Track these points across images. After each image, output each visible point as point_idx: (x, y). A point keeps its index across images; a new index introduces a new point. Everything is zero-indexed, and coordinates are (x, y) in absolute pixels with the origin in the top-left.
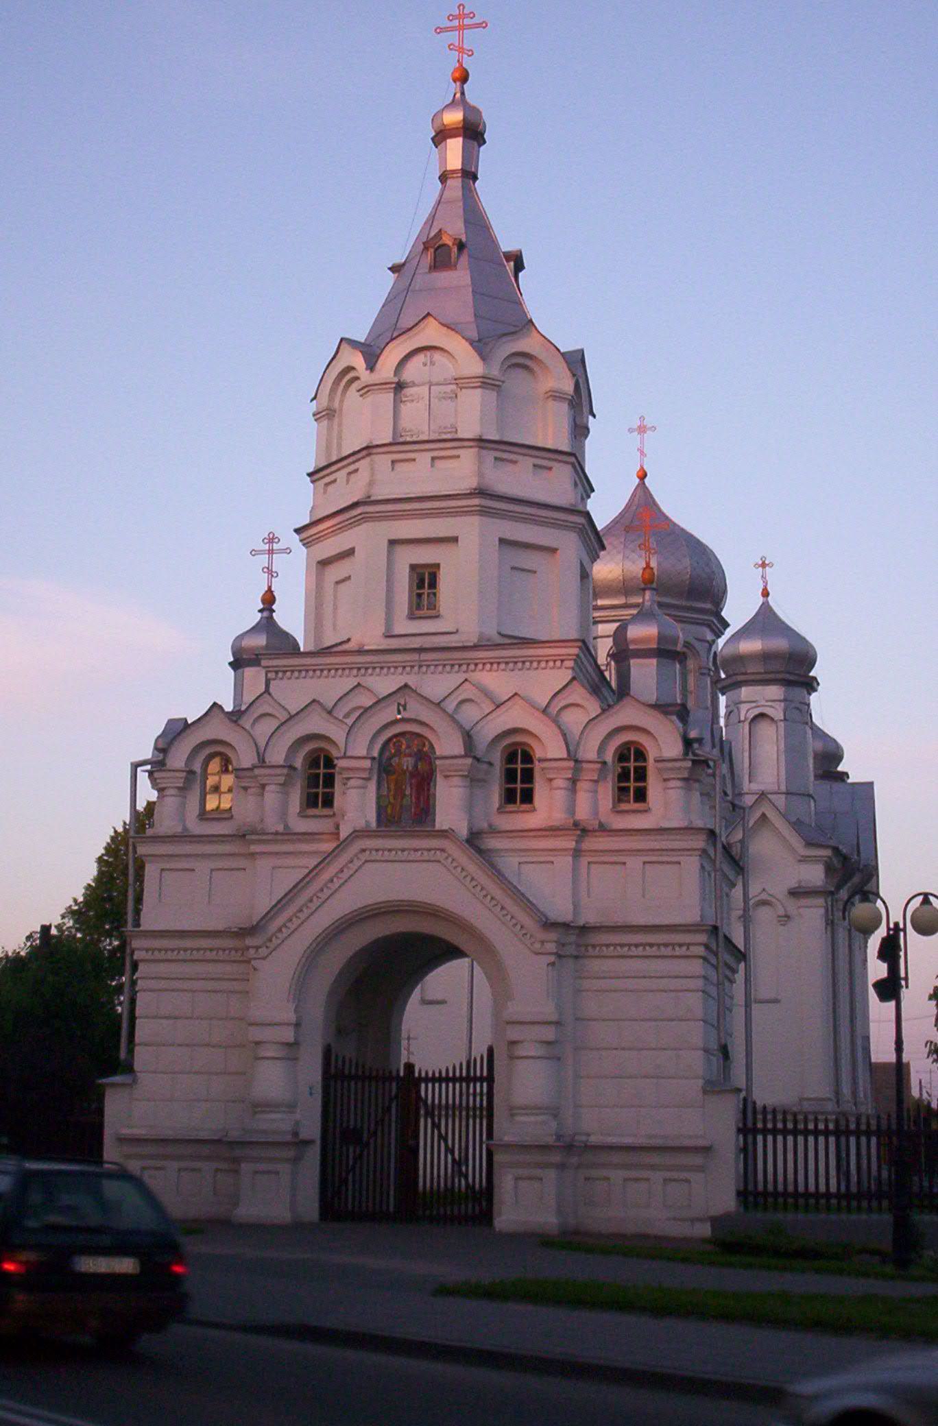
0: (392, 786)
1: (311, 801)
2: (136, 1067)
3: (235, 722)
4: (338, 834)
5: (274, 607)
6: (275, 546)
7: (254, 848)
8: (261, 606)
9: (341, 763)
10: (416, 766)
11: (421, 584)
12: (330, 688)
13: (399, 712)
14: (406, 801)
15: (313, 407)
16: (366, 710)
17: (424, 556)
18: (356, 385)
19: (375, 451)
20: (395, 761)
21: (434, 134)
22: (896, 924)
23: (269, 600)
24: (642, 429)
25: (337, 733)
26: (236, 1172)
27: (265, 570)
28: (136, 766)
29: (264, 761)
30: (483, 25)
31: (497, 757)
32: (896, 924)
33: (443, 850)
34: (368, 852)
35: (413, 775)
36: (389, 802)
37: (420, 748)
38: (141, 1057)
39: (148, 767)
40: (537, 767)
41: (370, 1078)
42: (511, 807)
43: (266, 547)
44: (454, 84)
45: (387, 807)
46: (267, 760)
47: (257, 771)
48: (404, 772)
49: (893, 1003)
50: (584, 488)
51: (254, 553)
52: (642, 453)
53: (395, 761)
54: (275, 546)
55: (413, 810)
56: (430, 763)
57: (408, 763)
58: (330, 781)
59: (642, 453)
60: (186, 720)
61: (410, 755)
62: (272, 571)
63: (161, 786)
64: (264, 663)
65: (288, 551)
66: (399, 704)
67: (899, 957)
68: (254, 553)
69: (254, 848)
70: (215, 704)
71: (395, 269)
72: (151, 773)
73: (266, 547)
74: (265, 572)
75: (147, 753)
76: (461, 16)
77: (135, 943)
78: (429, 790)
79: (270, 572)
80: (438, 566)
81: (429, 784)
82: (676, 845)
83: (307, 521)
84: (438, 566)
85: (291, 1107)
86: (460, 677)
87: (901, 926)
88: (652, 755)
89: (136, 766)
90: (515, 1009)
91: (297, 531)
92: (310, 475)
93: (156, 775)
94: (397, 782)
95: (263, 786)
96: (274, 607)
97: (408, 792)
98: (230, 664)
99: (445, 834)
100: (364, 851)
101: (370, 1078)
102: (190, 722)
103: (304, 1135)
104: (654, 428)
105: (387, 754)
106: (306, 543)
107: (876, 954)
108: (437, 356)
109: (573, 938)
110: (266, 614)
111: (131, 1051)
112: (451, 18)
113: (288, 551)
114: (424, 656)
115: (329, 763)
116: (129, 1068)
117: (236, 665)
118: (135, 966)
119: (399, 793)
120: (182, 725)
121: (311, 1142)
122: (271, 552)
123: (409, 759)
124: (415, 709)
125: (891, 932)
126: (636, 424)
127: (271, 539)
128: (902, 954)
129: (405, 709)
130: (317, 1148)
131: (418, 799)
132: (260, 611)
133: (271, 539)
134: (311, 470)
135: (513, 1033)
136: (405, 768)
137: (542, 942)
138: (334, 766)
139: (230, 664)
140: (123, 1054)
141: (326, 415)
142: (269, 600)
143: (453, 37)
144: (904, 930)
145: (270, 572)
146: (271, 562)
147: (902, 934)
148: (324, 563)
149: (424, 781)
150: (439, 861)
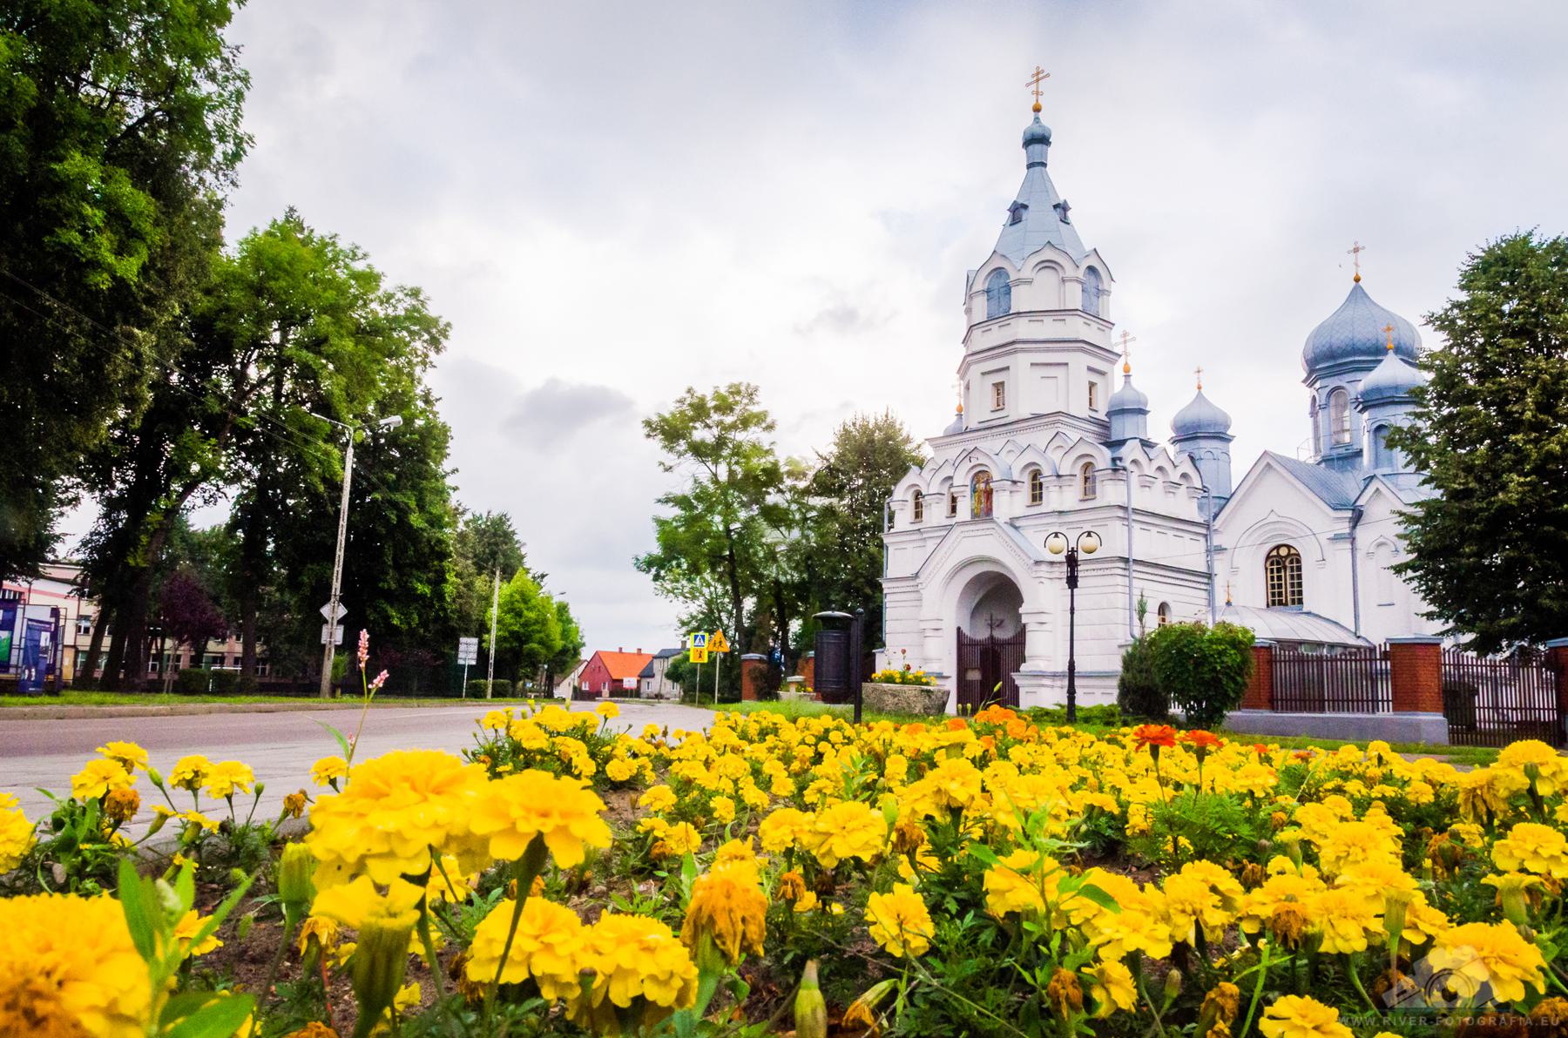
7: (925, 536)
17: (997, 378)
24: (1356, 250)
30: (1048, 75)
52: (1357, 265)
57: (982, 486)
59: (1357, 265)
69: (925, 536)
76: (1038, 73)
104: (1363, 248)
112: (1033, 76)
116: (884, 645)
119: (979, 502)
121: (947, 677)
126: (1360, 245)
141: (968, 311)
143: (1033, 87)
149: (989, 494)
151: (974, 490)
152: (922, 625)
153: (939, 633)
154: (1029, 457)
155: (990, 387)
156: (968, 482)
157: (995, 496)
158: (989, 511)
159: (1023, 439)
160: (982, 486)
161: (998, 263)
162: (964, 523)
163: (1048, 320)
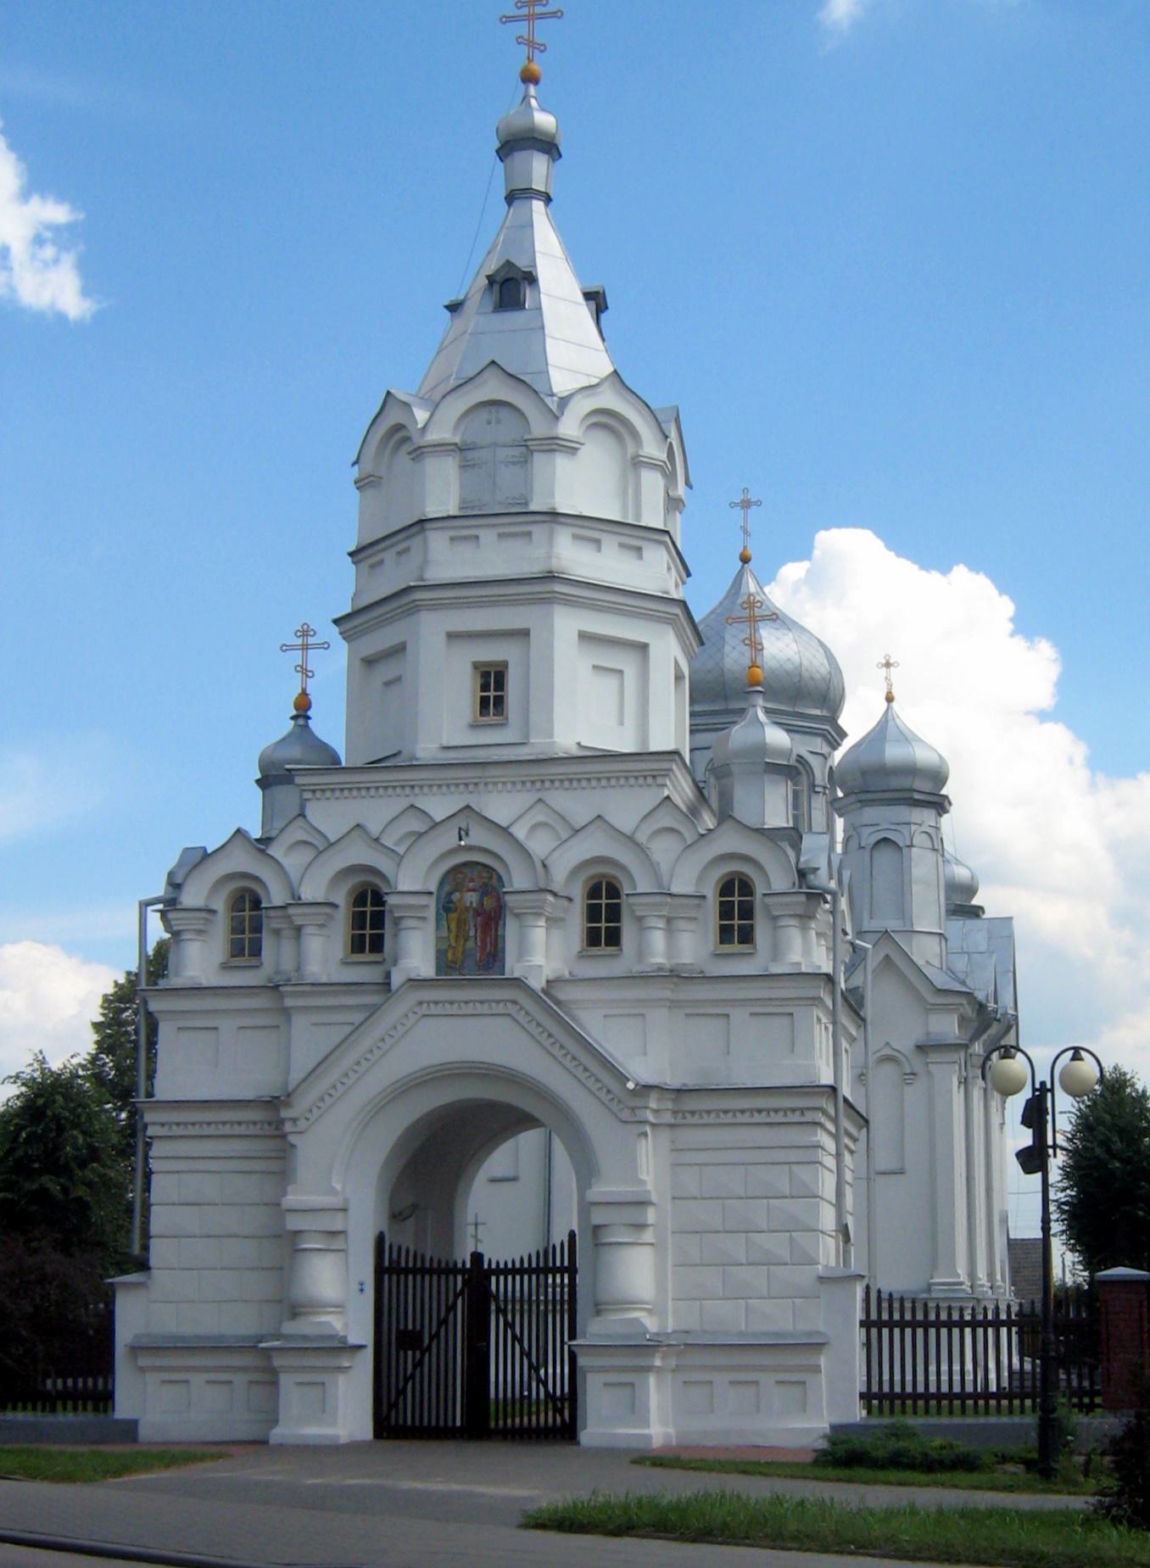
0: (453, 926)
1: (357, 945)
2: (153, 1262)
3: (262, 851)
4: (389, 984)
5: (310, 713)
6: (311, 640)
8: (294, 712)
9: (391, 900)
10: (481, 903)
11: (485, 687)
12: (376, 812)
13: (460, 839)
14: (470, 944)
15: (355, 472)
16: (420, 835)
17: (490, 653)
18: (407, 448)
19: (428, 525)
20: (456, 896)
21: (497, 145)
22: (1043, 1084)
23: (303, 707)
25: (383, 863)
26: (275, 1384)
27: (299, 669)
28: (144, 905)
29: (300, 898)
31: (578, 892)
32: (1043, 1084)
33: (514, 1002)
34: (425, 1005)
35: (477, 913)
36: (450, 946)
37: (486, 881)
38: (159, 1252)
39: (160, 906)
40: (625, 902)
41: (431, 1271)
42: (595, 950)
43: (300, 641)
44: (522, 86)
45: (446, 951)
46: (303, 897)
47: (291, 911)
48: (467, 909)
49: (1039, 1175)
50: (678, 571)
51: (285, 648)
53: (456, 896)
54: (311, 640)
55: (478, 955)
56: (499, 899)
57: (471, 898)
58: (378, 920)
60: (204, 849)
61: (473, 890)
62: (307, 671)
63: (175, 928)
64: (299, 780)
65: (325, 646)
66: (460, 829)
67: (1046, 1121)
68: (285, 648)
70: (239, 831)
71: (454, 308)
72: (163, 913)
73: (300, 641)
74: (298, 672)
75: (159, 889)
77: (148, 1118)
78: (496, 930)
79: (304, 671)
80: (505, 664)
81: (497, 924)
82: (791, 993)
83: (349, 610)
84: (505, 664)
85: (339, 1307)
86: (533, 797)
87: (1049, 1086)
88: (760, 889)
89: (144, 905)
90: (598, 1191)
91: (336, 622)
92: (351, 554)
93: (171, 915)
94: (459, 921)
95: (298, 930)
96: (310, 713)
97: (472, 933)
98: (258, 781)
99: (518, 983)
100: (420, 1003)
101: (431, 1271)
102: (209, 851)
103: (353, 1340)
105: (447, 888)
106: (346, 636)
107: (1020, 1119)
108: (504, 413)
109: (670, 1105)
110: (301, 722)
111: (146, 1248)
113: (325, 646)
114: (492, 771)
115: (378, 899)
116: (143, 1265)
117: (264, 783)
118: (148, 1145)
119: (461, 934)
120: (199, 855)
121: (361, 1347)
122: (305, 647)
123: (473, 894)
124: (478, 837)
125: (1037, 1093)
127: (305, 632)
128: (1049, 1118)
129: (467, 834)
130: (368, 1355)
131: (484, 942)
132: (293, 718)
133: (305, 632)
134: (352, 548)
135: (598, 1217)
136: (468, 904)
137: (633, 1109)
138: (383, 904)
139: (258, 781)
140: (136, 1250)
142: (303, 707)
144: (1052, 1090)
145: (304, 671)
146: (305, 659)
147: (1049, 1095)
148: (370, 662)
149: (491, 919)
150: (509, 1015)
151: (447, 908)
152: (293, 1223)
153: (338, 1243)
154: (593, 846)
155: (469, 669)
156: (433, 887)
157: (511, 930)
158: (492, 957)
159: (576, 805)
160: (471, 898)
161: (493, 389)
162: (415, 983)
163: (610, 543)
